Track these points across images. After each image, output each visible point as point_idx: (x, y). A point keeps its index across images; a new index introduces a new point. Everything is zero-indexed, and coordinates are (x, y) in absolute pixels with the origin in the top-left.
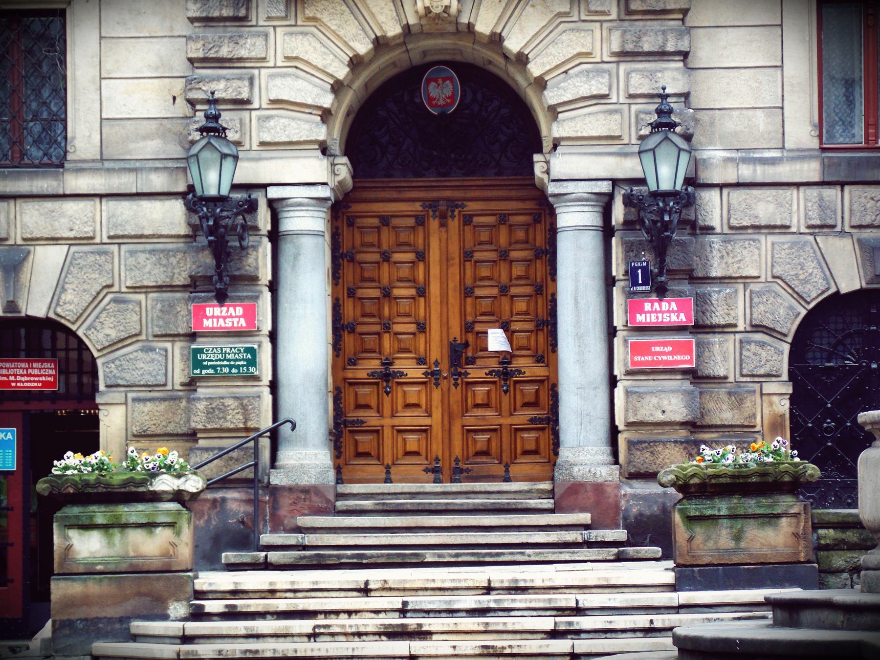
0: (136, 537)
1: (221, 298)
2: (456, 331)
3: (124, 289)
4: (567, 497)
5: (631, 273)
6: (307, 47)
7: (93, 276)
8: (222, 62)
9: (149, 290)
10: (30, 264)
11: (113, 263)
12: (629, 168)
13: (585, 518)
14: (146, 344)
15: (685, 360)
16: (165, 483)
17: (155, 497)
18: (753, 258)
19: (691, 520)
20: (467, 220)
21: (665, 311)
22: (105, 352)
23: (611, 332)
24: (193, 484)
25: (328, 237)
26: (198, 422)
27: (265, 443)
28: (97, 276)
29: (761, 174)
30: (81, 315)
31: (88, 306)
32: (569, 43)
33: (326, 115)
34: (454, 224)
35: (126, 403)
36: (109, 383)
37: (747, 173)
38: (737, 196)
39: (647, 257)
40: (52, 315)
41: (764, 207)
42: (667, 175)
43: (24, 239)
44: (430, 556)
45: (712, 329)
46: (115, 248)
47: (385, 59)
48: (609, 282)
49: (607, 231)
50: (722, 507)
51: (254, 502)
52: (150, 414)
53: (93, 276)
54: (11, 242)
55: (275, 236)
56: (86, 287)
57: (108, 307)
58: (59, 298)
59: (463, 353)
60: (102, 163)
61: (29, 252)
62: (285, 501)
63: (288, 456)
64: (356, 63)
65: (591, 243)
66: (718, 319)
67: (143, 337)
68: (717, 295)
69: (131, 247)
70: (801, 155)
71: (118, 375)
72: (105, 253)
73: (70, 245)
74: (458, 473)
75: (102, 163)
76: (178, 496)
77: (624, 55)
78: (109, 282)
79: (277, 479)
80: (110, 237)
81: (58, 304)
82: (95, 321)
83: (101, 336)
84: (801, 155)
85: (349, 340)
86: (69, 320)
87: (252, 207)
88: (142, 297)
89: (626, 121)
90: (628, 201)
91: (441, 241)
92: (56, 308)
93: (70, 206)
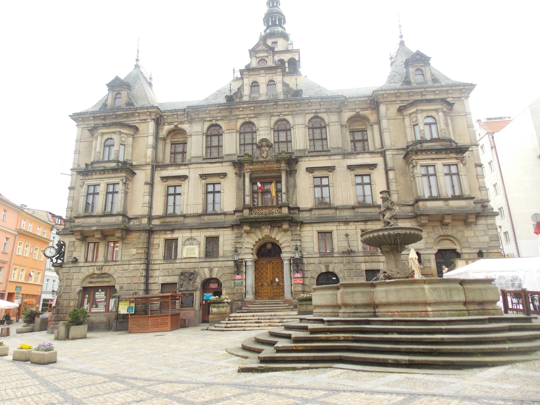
0: (221, 308)
1: (238, 274)
2: (272, 279)
4: (286, 302)
5: (294, 270)
6: (250, 240)
8: (238, 243)
12: (292, 255)
13: (288, 305)
15: (302, 282)
16: (225, 301)
17: (224, 303)
18: (310, 268)
19: (300, 305)
20: (273, 263)
21: (298, 275)
23: (291, 278)
24: (229, 301)
25: (254, 266)
26: (235, 292)
27: (244, 295)
29: (311, 256)
32: (284, 239)
33: (252, 249)
34: (271, 264)
37: (309, 256)
38: (308, 259)
39: (296, 268)
41: (312, 260)
42: (297, 256)
44: (265, 311)
45: (305, 278)
47: (261, 242)
48: (291, 271)
49: (290, 264)
50: (304, 303)
51: (242, 303)
52: (229, 291)
55: (246, 266)
59: (273, 281)
60: (223, 257)
62: (246, 303)
63: (247, 297)
64: (256, 242)
65: (288, 266)
66: (306, 276)
68: (306, 273)
70: (316, 253)
74: (272, 299)
75: (223, 257)
76: (227, 302)
77: (292, 240)
79: (245, 300)
84: (316, 253)
85: (257, 280)
87: (242, 262)
89: (292, 249)
90: (293, 260)
91: (269, 266)
93: (219, 262)
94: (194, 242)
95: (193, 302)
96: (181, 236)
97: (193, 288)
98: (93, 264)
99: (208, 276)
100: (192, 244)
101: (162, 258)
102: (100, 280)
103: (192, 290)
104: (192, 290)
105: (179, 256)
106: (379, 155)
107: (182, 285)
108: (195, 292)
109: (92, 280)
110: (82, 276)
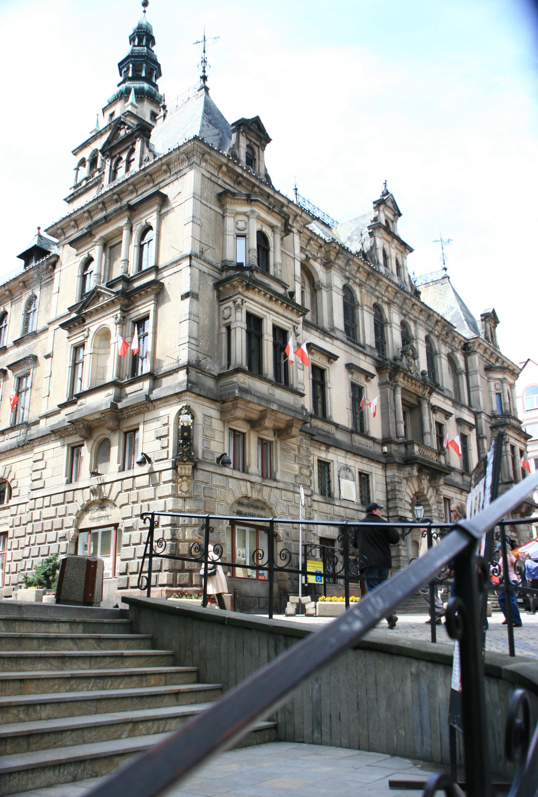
94: (350, 475)
96: (337, 459)
98: (245, 476)
100: (347, 478)
101: (317, 490)
102: (251, 511)
105: (336, 495)
106: (472, 415)
109: (241, 509)
110: (231, 499)
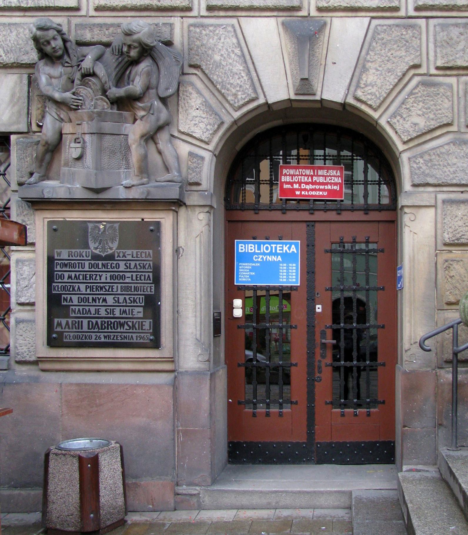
3: (433, 71)
7: (398, 53)
9: (461, 72)
10: (326, 38)
11: (420, 39)
14: (457, 136)
22: (411, 144)
28: (404, 54)
30: (385, 99)
31: (392, 90)
35: (435, 206)
36: (417, 182)
40: (351, 100)
43: (320, 9)
46: (422, 22)
53: (398, 53)
54: (304, 13)
56: (389, 66)
57: (416, 91)
58: (360, 79)
61: (325, 24)
67: (454, 128)
69: (441, 21)
71: (427, 171)
72: (412, 26)
73: (373, 18)
78: (416, 62)
80: (417, 9)
81: (358, 86)
82: (400, 107)
83: (407, 126)
86: (370, 106)
88: (453, 80)
92: (356, 90)
95: (152, 304)
97: (161, 187)
99: (278, 89)
103: (149, 203)
104: (149, 203)
107: (54, 148)
108: (166, 220)
